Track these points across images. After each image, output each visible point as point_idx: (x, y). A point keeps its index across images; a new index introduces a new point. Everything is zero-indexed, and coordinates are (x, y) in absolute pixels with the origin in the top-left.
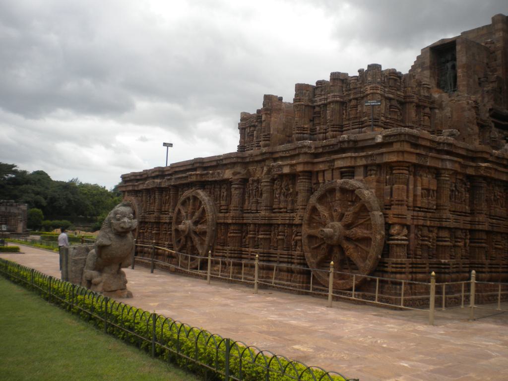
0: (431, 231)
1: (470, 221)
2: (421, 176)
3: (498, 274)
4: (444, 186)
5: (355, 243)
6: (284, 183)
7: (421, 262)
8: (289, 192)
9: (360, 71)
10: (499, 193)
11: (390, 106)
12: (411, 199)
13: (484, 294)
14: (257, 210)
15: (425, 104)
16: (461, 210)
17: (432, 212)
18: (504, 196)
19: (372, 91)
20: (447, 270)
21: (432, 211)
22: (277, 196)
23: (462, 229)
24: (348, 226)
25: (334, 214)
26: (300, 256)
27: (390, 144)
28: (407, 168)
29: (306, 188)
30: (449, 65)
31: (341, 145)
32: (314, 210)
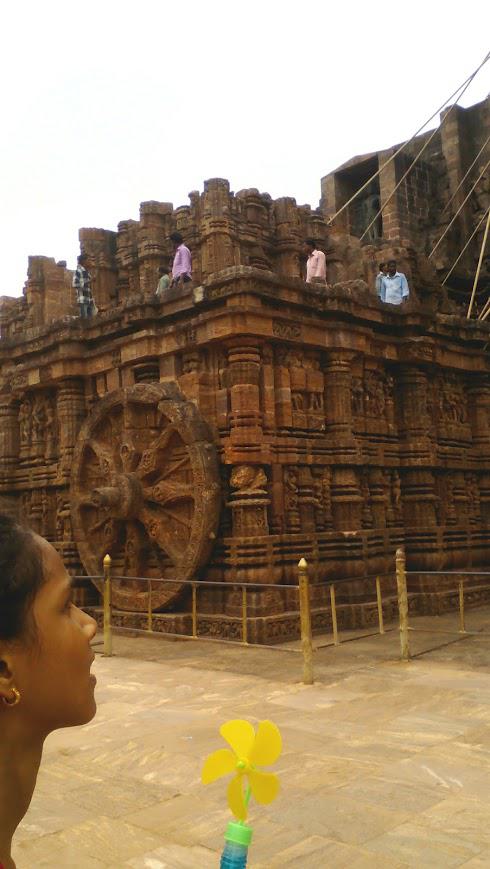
0: (319, 476)
1: (399, 452)
2: (289, 366)
4: (338, 384)
5: (166, 511)
6: (35, 407)
9: (193, 196)
10: (454, 396)
11: (250, 258)
12: (270, 413)
13: (438, 594)
16: (378, 431)
17: (318, 437)
18: (466, 402)
19: (212, 230)
22: (25, 433)
23: (383, 469)
24: (152, 478)
25: (124, 457)
26: (71, 550)
27: (221, 302)
28: (257, 350)
29: (75, 412)
30: (369, 202)
31: (130, 317)
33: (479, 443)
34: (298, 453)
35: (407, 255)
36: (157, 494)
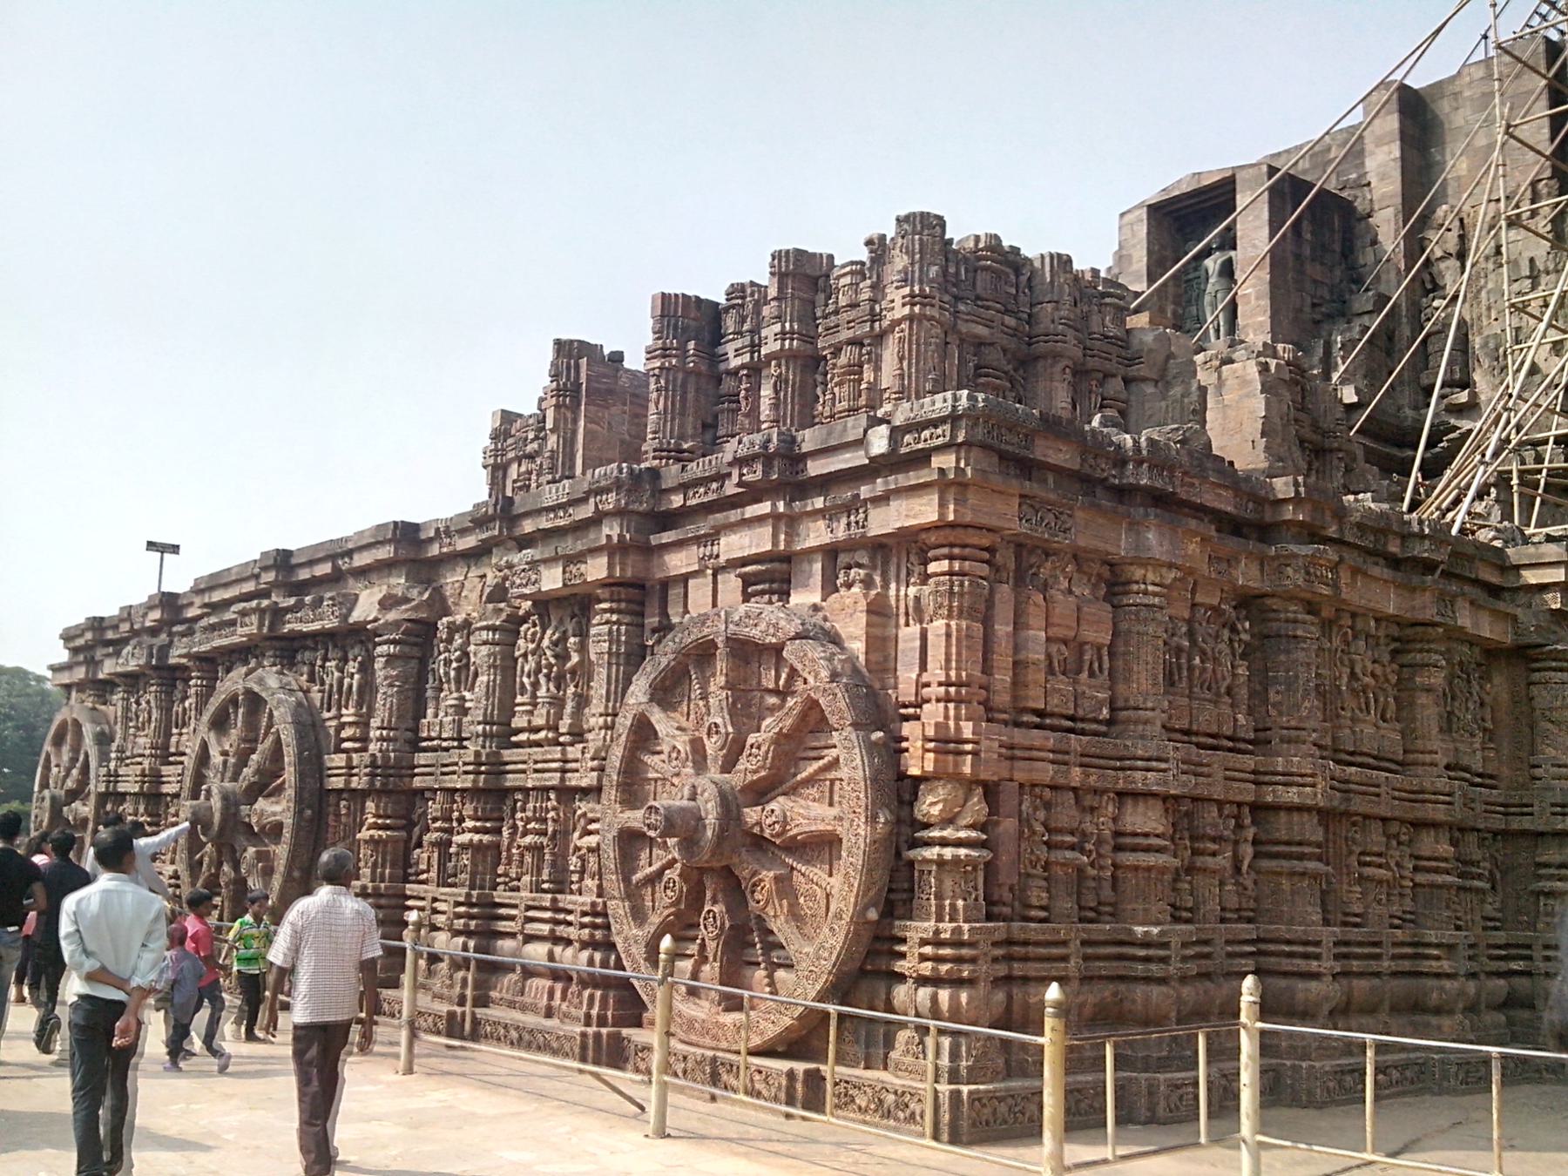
1: (1254, 772)
2: (1045, 588)
3: (1376, 982)
4: (1141, 628)
8: (569, 665)
11: (977, 367)
12: (1003, 678)
13: (1317, 1064)
15: (1108, 366)
16: (1214, 729)
17: (1096, 734)
18: (1394, 679)
20: (1155, 969)
21: (1094, 726)
22: (525, 680)
23: (1220, 804)
24: (760, 792)
25: (711, 745)
28: (986, 555)
30: (1212, 264)
31: (741, 475)
33: (1415, 763)
34: (1053, 762)
36: (769, 821)
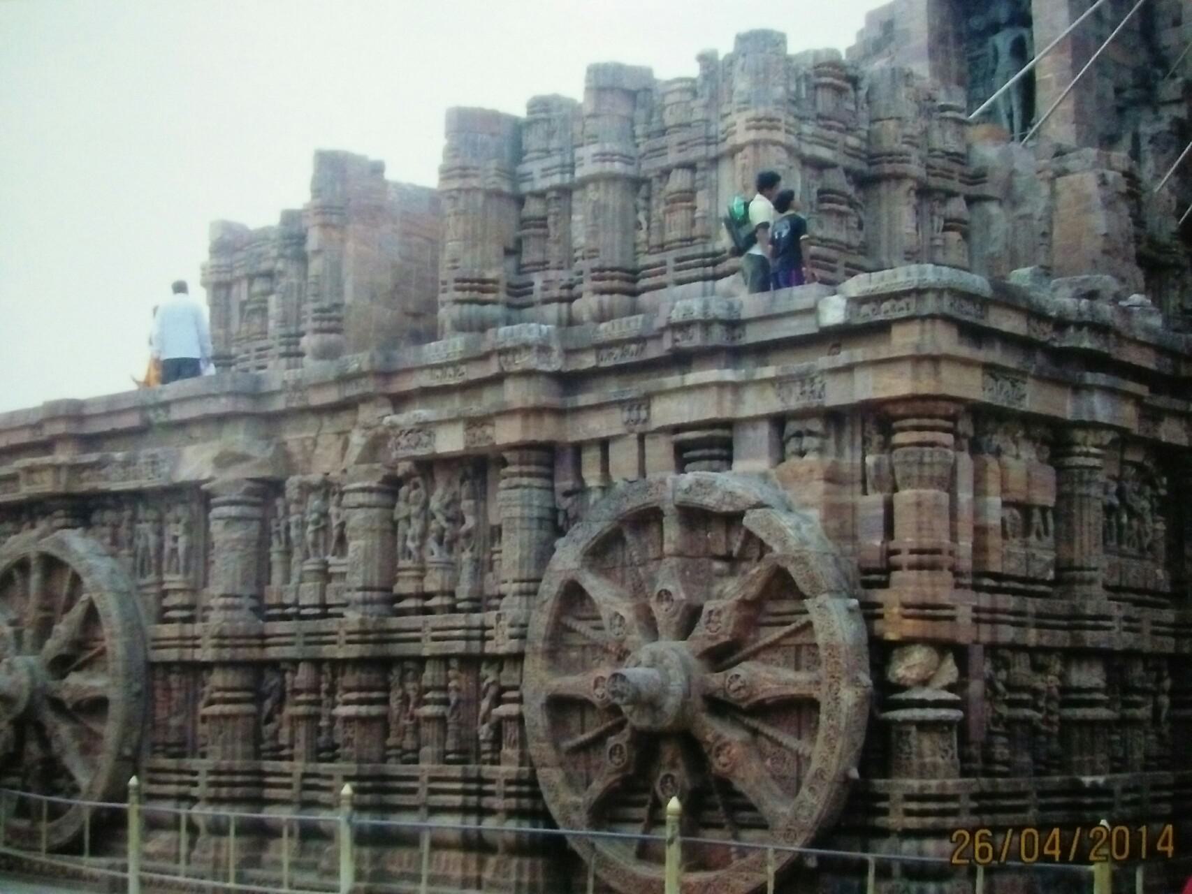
0: (1038, 668)
2: (998, 453)
4: (1084, 490)
5: (747, 720)
6: (439, 492)
7: (1010, 790)
8: (463, 529)
9: (706, 60)
11: (820, 192)
12: (965, 544)
14: (327, 607)
16: (1140, 584)
19: (752, 135)
21: (1042, 588)
22: (411, 545)
24: (719, 657)
25: (660, 611)
26: (518, 782)
27: (881, 329)
28: (949, 424)
29: (536, 513)
30: (1002, 41)
32: (573, 595)
34: (1013, 624)
35: (1123, 187)
36: (733, 687)
